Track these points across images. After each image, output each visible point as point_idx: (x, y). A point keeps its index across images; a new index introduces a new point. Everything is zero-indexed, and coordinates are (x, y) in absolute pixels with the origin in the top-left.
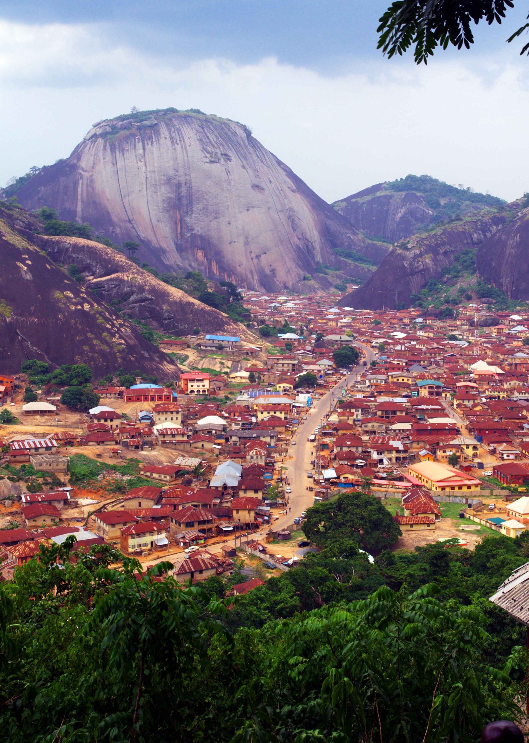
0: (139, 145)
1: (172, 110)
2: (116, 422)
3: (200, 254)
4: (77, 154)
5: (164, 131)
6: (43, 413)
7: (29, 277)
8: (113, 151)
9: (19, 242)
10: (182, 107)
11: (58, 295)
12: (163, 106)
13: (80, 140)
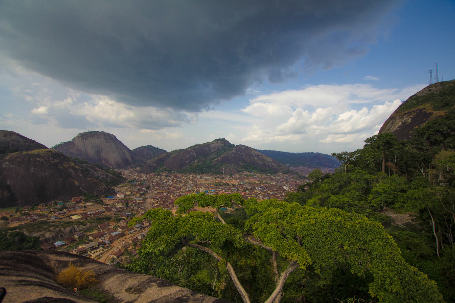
0: (90, 139)
1: (97, 131)
2: (109, 206)
3: (104, 161)
4: (74, 139)
5: (96, 136)
6: (91, 205)
7: (81, 175)
8: (83, 140)
9: (78, 167)
10: (100, 131)
11: (89, 179)
12: (96, 130)
13: (75, 136)
